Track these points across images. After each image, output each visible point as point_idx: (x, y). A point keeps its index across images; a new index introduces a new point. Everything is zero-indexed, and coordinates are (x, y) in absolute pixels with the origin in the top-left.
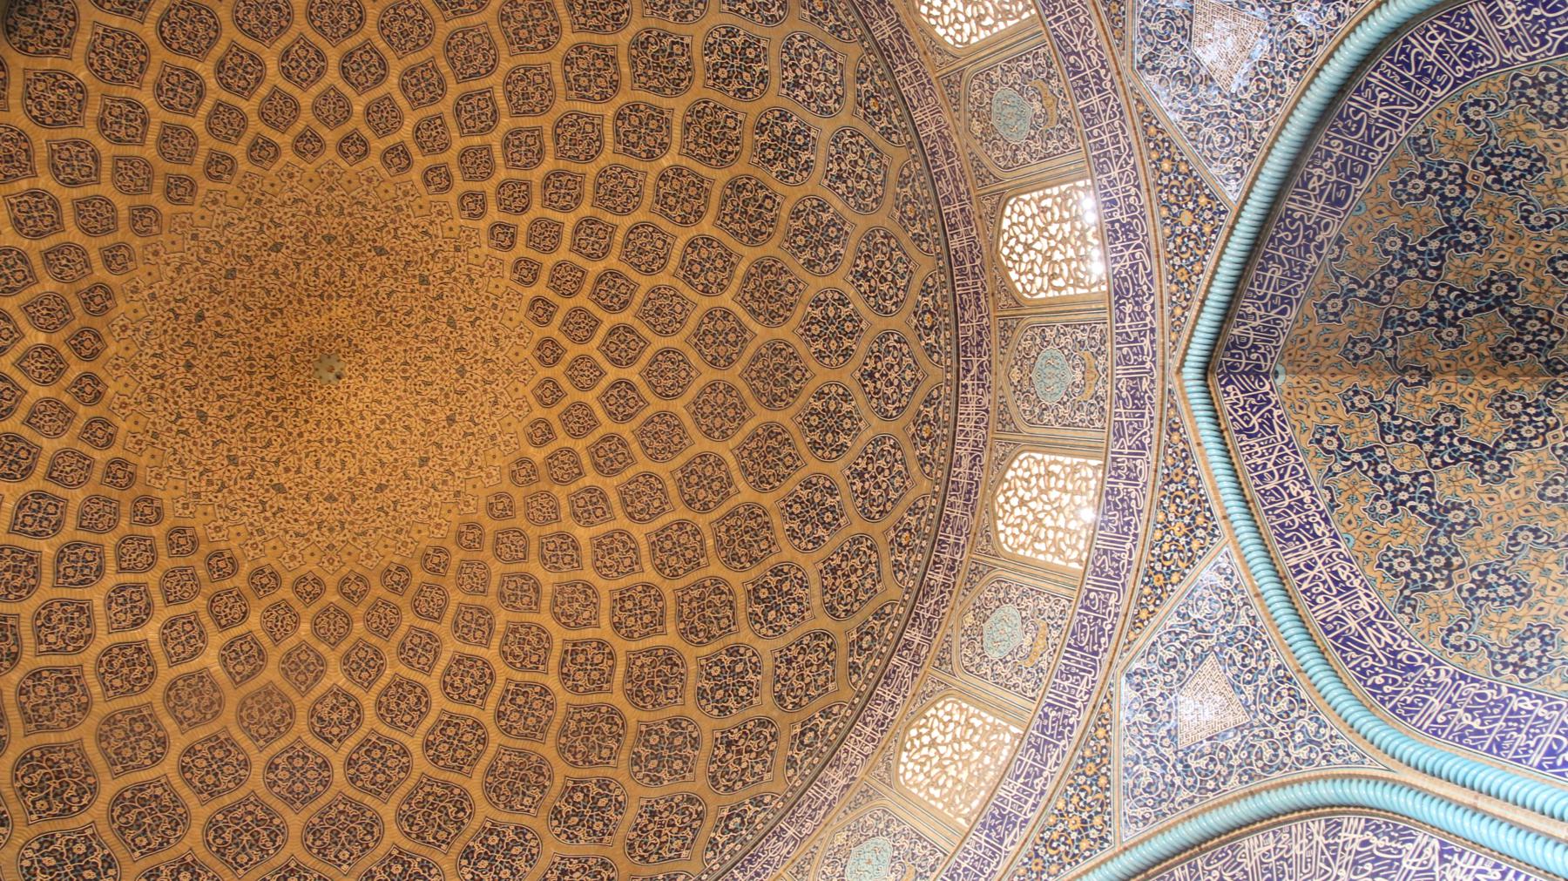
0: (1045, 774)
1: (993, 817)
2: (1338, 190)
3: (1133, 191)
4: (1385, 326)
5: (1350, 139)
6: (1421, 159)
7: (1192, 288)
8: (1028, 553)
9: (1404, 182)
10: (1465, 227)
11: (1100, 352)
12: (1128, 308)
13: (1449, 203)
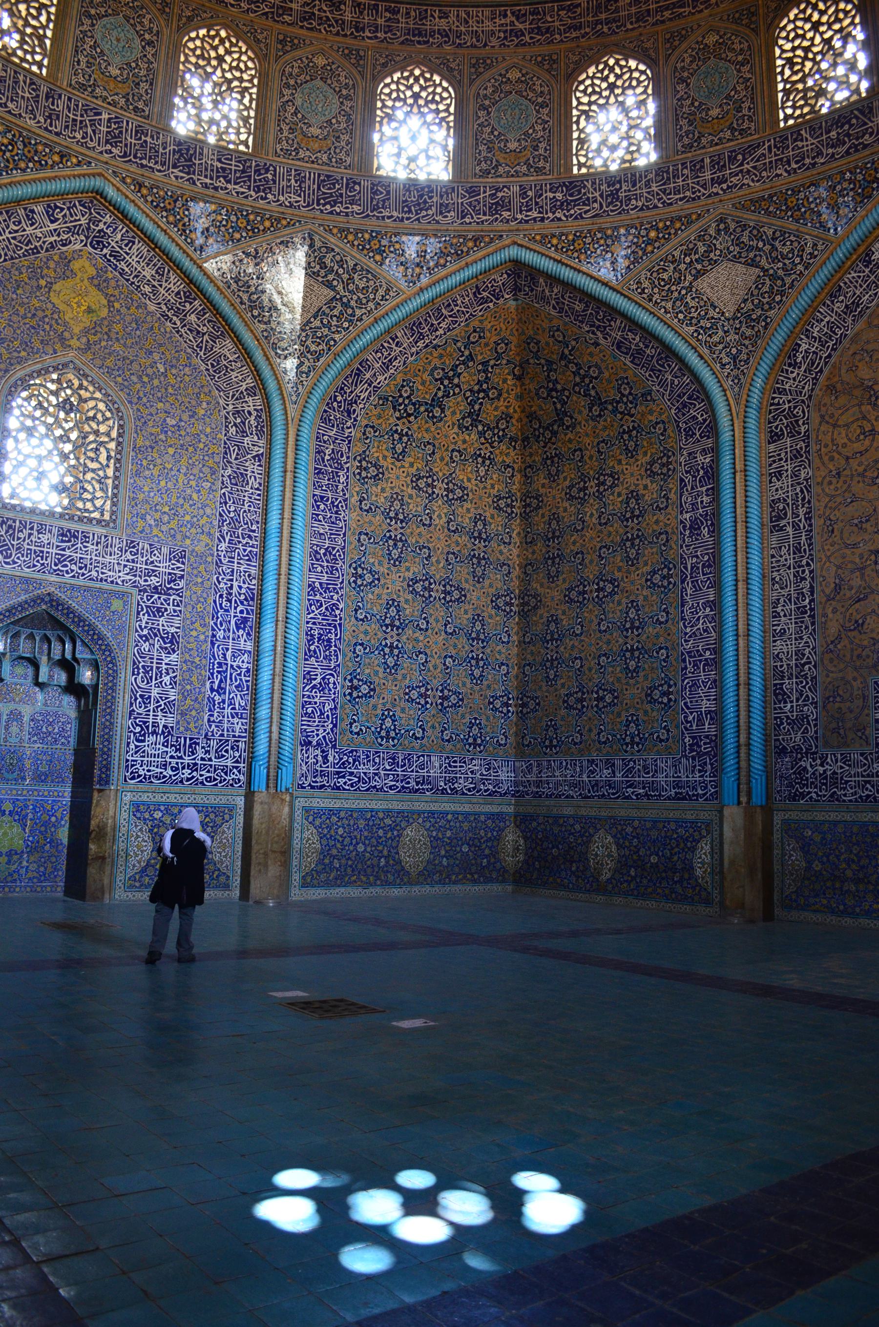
0: (229, 186)
1: (188, 150)
3: (640, 204)
5: (655, 360)
7: (570, 253)
8: (379, 112)
9: (628, 384)
11: (529, 166)
12: (559, 196)
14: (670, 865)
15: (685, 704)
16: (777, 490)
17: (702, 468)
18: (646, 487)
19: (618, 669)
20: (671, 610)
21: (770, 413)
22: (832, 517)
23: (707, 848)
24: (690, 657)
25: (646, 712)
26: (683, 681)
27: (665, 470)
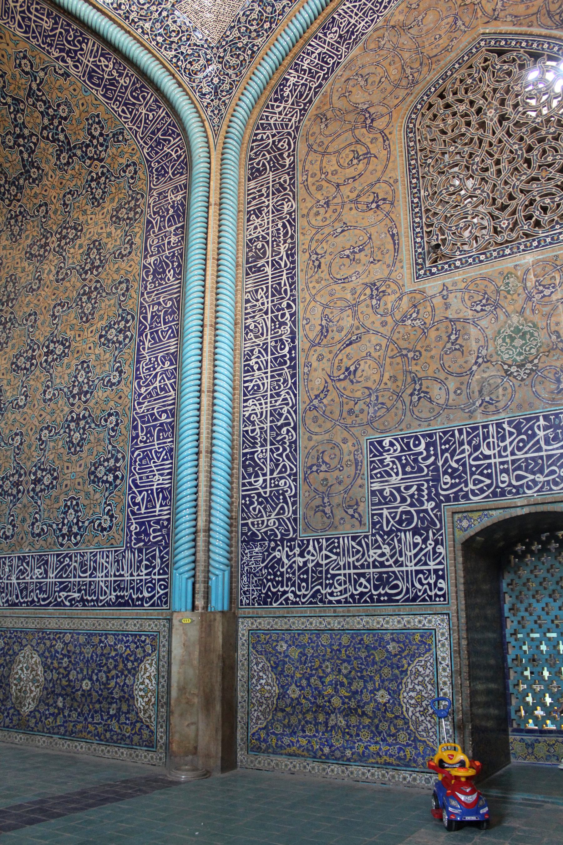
2: (98, 78)
4: (14, 99)
5: (129, 91)
6: (111, 135)
9: (99, 123)
10: (70, 157)
13: (84, 149)
14: (105, 693)
15: (134, 481)
16: (256, 228)
17: (173, 207)
18: (109, 235)
19: (60, 443)
20: (125, 368)
21: (252, 149)
22: (319, 251)
23: (152, 670)
24: (143, 422)
25: (87, 494)
26: (133, 453)
27: (131, 215)
